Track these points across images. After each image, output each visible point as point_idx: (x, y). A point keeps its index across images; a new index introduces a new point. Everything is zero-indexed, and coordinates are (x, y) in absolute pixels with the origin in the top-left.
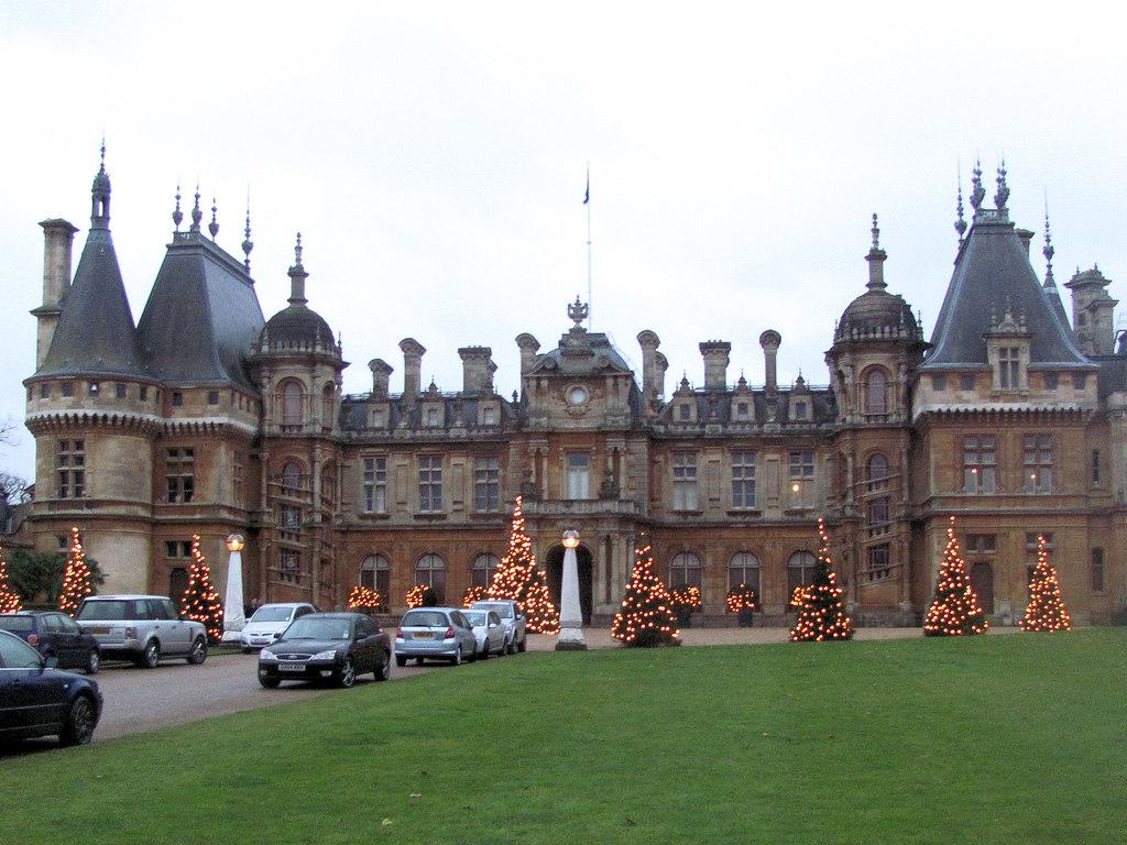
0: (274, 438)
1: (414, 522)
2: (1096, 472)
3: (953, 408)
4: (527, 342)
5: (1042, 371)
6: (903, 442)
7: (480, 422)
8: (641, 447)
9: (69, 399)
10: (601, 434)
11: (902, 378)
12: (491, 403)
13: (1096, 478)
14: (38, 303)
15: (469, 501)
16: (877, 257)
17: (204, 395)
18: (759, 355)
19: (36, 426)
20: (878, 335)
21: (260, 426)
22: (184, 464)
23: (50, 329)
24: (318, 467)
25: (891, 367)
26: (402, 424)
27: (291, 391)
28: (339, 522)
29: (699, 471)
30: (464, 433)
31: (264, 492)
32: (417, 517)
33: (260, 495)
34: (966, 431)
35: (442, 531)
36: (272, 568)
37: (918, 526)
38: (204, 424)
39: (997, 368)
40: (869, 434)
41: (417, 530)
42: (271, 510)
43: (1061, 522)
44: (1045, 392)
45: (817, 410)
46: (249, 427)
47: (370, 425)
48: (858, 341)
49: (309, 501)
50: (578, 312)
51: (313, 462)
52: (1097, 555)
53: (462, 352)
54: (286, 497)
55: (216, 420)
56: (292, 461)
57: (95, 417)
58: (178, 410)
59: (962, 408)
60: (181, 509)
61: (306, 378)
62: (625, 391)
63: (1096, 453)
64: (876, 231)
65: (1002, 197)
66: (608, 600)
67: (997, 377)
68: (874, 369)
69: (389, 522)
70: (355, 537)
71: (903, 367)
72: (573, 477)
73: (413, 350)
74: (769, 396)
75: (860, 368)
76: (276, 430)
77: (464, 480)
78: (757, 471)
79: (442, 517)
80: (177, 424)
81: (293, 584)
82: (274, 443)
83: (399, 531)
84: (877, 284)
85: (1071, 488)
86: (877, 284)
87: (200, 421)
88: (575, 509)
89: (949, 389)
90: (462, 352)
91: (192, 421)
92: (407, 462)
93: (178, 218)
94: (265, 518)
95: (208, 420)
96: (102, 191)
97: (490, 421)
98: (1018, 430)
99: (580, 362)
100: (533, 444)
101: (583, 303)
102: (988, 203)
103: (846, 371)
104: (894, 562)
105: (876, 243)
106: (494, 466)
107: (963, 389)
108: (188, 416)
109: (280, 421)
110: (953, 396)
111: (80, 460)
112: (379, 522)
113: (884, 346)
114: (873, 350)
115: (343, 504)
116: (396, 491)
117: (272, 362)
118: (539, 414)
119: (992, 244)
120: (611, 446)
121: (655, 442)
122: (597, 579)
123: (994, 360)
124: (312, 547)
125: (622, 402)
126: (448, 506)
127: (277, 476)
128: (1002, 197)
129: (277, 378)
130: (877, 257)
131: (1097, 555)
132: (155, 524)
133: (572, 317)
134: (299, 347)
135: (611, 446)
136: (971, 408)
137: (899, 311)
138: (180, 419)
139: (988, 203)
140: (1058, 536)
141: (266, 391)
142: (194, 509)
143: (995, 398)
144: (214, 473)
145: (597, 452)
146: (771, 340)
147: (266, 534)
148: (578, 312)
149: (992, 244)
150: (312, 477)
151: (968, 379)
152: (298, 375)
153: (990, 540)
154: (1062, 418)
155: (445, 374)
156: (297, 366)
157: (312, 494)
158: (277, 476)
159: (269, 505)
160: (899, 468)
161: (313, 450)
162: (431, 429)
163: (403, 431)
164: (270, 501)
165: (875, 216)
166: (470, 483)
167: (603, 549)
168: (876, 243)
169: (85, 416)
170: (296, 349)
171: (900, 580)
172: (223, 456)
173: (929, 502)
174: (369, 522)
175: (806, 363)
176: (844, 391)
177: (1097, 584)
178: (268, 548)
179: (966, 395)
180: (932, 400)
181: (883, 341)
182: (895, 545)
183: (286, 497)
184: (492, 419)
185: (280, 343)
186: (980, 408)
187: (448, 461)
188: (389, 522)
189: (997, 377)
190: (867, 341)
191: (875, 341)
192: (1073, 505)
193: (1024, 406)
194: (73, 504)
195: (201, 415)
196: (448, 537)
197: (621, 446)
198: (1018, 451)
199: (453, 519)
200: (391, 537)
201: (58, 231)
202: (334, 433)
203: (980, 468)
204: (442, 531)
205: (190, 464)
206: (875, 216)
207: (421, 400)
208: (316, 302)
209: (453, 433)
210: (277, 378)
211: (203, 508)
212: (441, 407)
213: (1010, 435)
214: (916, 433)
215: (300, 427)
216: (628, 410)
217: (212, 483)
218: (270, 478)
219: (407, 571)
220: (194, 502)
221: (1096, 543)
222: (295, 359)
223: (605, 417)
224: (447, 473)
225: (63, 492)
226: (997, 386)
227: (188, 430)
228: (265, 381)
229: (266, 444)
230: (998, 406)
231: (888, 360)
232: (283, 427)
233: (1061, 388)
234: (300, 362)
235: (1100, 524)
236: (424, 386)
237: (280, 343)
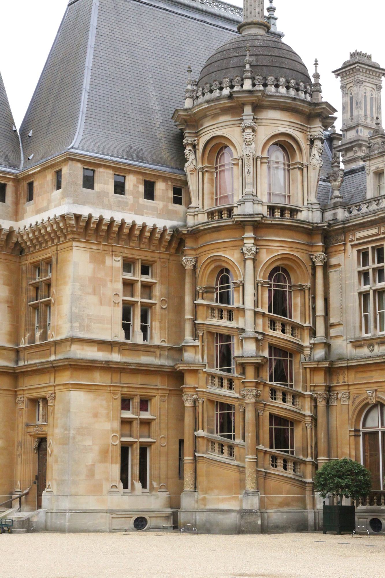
0: (196, 233)
17: (50, 176)
28: (320, 353)
31: (188, 316)
36: (200, 433)
42: (197, 343)
46: (157, 216)
54: (215, 321)
58: (29, 207)
61: (233, 133)
70: (351, 377)
108: (38, 212)
109: (208, 206)
115: (328, 326)
127: (208, 290)
132: (15, 375)
134: (221, 89)
152: (223, 132)
156: (222, 119)
158: (208, 290)
159: (195, 336)
164: (195, 327)
170: (217, 93)
174: (365, 351)
178: (195, 401)
183: (215, 321)
195: (47, 209)
202: (302, 216)
215: (230, 210)
218: (195, 295)
222: (234, 107)
234: (225, 111)
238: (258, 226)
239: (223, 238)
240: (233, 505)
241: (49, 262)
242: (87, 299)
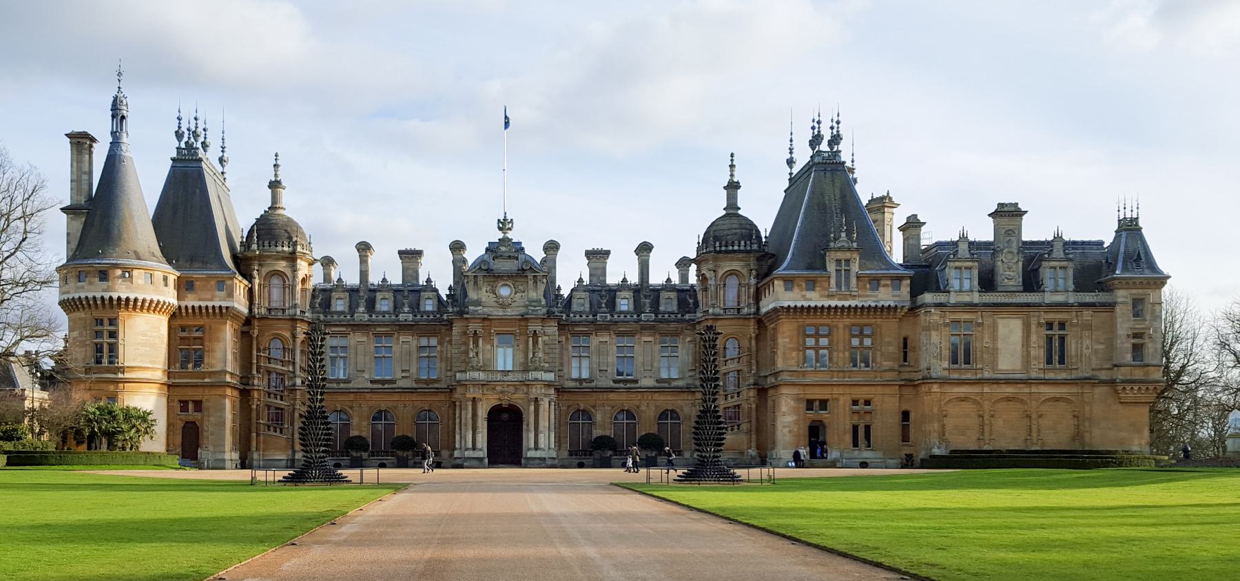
0: (262, 318)
1: (370, 385)
2: (905, 353)
3: (799, 305)
4: (457, 247)
5: (868, 276)
6: (752, 328)
7: (422, 309)
8: (552, 329)
9: (104, 284)
10: (524, 319)
11: (753, 281)
12: (431, 294)
13: (905, 360)
14: (67, 203)
15: (413, 370)
16: (733, 187)
17: (213, 283)
18: (634, 260)
19: (68, 305)
20: (736, 248)
21: (250, 309)
22: (195, 338)
23: (79, 224)
24: (299, 341)
25: (745, 272)
26: (361, 309)
27: (276, 281)
29: (593, 348)
30: (411, 317)
32: (372, 382)
33: (251, 364)
34: (808, 321)
35: (393, 391)
37: (762, 392)
38: (207, 307)
39: (834, 275)
40: (727, 322)
41: (372, 391)
43: (879, 390)
44: (868, 293)
45: (682, 304)
47: (333, 309)
48: (720, 252)
49: (291, 368)
50: (504, 225)
51: (294, 337)
52: (906, 415)
53: (400, 253)
55: (224, 304)
56: (278, 337)
57: (128, 299)
59: (806, 304)
60: (192, 375)
61: (288, 272)
62: (542, 287)
63: (905, 339)
64: (732, 166)
66: (536, 448)
67: (833, 281)
68: (732, 273)
69: (351, 385)
71: (754, 272)
72: (500, 350)
73: (364, 248)
75: (720, 273)
76: (263, 311)
77: (410, 353)
78: (636, 347)
79: (393, 382)
80: (190, 306)
81: (278, 434)
82: (263, 322)
83: (359, 392)
84: (732, 206)
85: (887, 364)
86: (732, 206)
87: (210, 304)
88: (510, 377)
89: (796, 289)
90: (400, 253)
91: (203, 304)
92: (365, 339)
93: (179, 135)
94: (256, 382)
95: (217, 304)
97: (429, 308)
98: (848, 321)
99: (506, 262)
100: (472, 327)
101: (509, 218)
102: (824, 147)
103: (709, 274)
104: (743, 419)
105: (732, 175)
106: (434, 342)
107: (807, 290)
110: (799, 296)
111: (113, 335)
112: (342, 385)
113: (740, 256)
114: (732, 260)
116: (355, 361)
117: (261, 259)
118: (478, 303)
120: (531, 328)
121: (562, 327)
122: (528, 431)
123: (831, 267)
124: (294, 405)
125: (537, 293)
126: (399, 375)
129: (264, 271)
130: (733, 187)
131: (906, 415)
133: (500, 229)
135: (531, 328)
136: (813, 304)
137: (750, 230)
138: (191, 301)
139: (824, 147)
140: (876, 401)
141: (257, 281)
142: (203, 375)
143: (831, 296)
144: (218, 347)
145: (521, 334)
147: (256, 395)
148: (504, 225)
150: (293, 351)
151: (811, 284)
153: (824, 404)
154: (856, 312)
155: (386, 269)
157: (294, 364)
159: (258, 372)
160: (750, 349)
161: (294, 328)
162: (384, 314)
163: (361, 314)
165: (732, 155)
166: (415, 356)
167: (532, 408)
168: (732, 175)
169: (119, 299)
170: (280, 248)
171: (749, 432)
172: (228, 334)
173: (776, 374)
176: (706, 290)
177: (905, 438)
179: (809, 294)
180: (780, 296)
181: (740, 251)
182: (745, 406)
184: (429, 306)
185: (266, 243)
186: (820, 305)
187: (398, 339)
188: (351, 385)
189: (833, 281)
190: (727, 252)
191: (734, 251)
192: (889, 376)
193: (853, 303)
194: (108, 371)
195: (211, 300)
196: (396, 397)
197: (538, 329)
198: (847, 336)
199: (401, 384)
200: (351, 397)
201: (81, 142)
203: (817, 348)
204: (393, 391)
205: (201, 338)
206: (732, 155)
207: (374, 291)
209: (402, 317)
210: (264, 271)
211: (211, 374)
212: (390, 295)
213: (841, 326)
214: (763, 324)
215: (284, 310)
216: (544, 302)
217: (219, 354)
218: (258, 350)
219: (365, 423)
220: (204, 368)
221: (905, 408)
223: (526, 306)
224: (396, 348)
225: (99, 361)
226: (833, 289)
227: (198, 311)
228: (255, 273)
229: (256, 323)
230: (833, 303)
231: (743, 267)
232: (269, 310)
233: (881, 289)
234: (283, 258)
235: (908, 391)
236: (422, 280)
237: (266, 243)
238: (293, 320)
239: (281, 324)
240: (283, 457)
241: (200, 328)
242: (225, 351)
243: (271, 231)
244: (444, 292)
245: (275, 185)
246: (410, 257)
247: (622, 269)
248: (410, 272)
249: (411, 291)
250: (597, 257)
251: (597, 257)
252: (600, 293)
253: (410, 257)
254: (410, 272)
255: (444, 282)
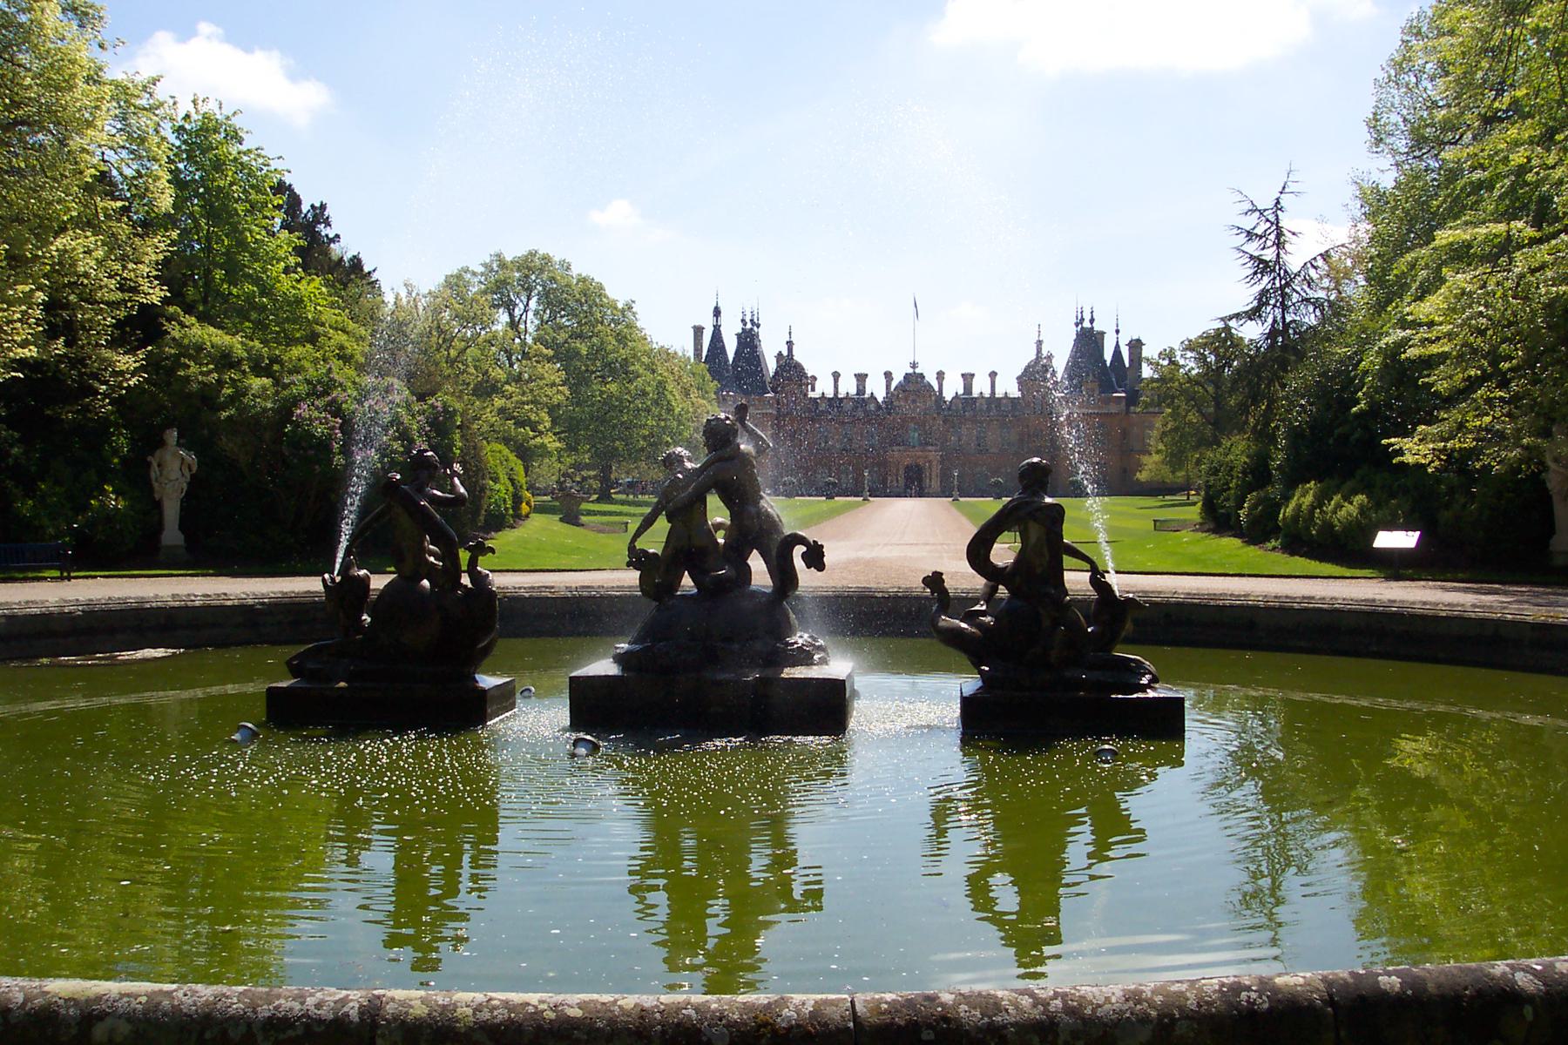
4: (888, 375)
16: (1040, 343)
50: (914, 366)
65: (1092, 321)
73: (836, 376)
74: (993, 401)
96: (717, 312)
119: (1089, 340)
128: (1092, 321)
130: (1040, 343)
146: (993, 375)
148: (914, 366)
149: (1089, 340)
175: (1009, 387)
184: (872, 407)
208: (798, 357)
243: (788, 365)
244: (880, 400)
245: (790, 344)
246: (861, 378)
247: (981, 387)
248: (861, 391)
249: (861, 401)
250: (968, 378)
251: (968, 378)
252: (967, 401)
253: (861, 378)
254: (861, 391)
255: (880, 396)
